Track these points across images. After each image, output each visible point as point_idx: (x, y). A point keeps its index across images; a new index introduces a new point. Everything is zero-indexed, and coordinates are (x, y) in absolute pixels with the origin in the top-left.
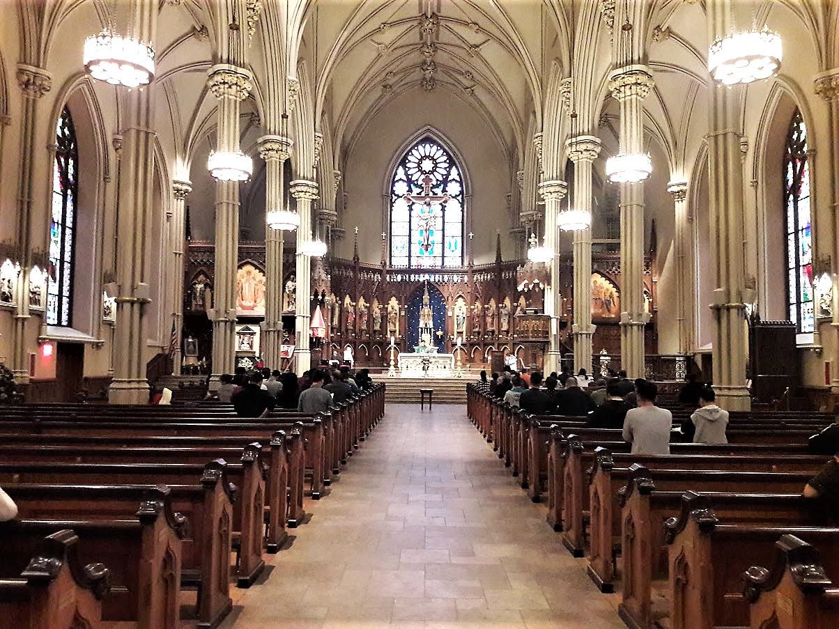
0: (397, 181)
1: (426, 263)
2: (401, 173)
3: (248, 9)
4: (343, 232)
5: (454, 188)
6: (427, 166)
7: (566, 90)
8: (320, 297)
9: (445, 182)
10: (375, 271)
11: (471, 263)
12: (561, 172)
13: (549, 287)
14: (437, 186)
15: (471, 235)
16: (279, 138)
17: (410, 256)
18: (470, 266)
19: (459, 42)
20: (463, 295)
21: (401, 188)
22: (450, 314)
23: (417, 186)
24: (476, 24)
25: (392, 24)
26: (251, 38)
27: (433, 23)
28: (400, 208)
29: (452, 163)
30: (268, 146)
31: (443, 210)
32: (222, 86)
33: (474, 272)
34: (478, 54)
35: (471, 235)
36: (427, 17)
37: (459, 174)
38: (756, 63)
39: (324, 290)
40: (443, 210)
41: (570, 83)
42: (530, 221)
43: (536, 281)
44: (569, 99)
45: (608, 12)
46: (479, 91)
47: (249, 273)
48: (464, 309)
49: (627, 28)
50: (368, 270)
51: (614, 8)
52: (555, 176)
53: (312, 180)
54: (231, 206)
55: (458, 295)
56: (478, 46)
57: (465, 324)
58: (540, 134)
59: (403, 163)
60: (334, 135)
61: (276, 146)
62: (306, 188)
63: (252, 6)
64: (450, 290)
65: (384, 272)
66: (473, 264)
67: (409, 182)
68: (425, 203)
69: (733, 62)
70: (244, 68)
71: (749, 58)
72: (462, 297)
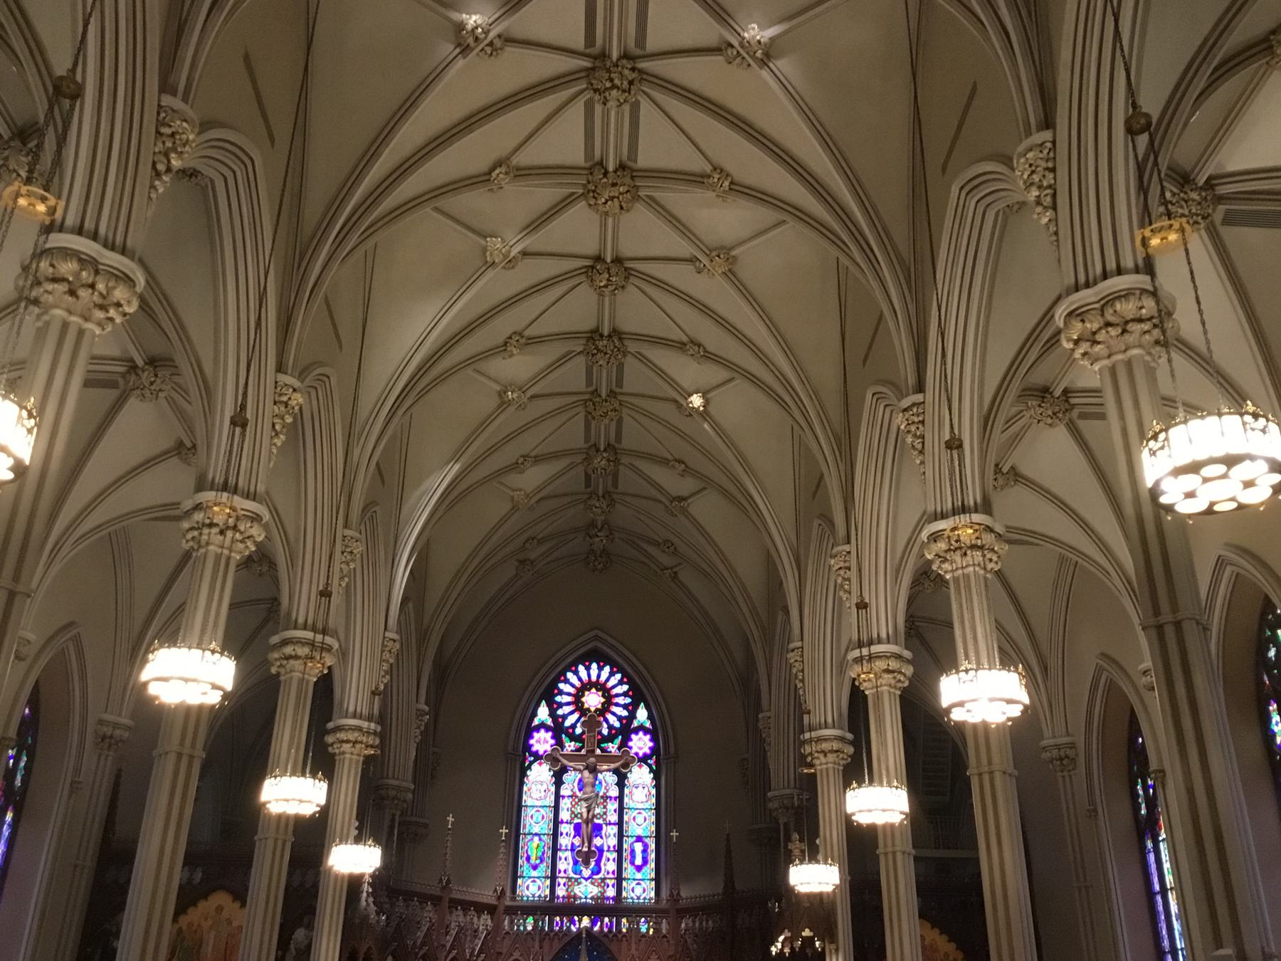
0: (537, 729)
1: (586, 891)
2: (543, 713)
3: (275, 403)
4: (425, 826)
5: (641, 744)
6: (593, 700)
7: (842, 564)
9: (626, 730)
10: (480, 908)
11: (675, 893)
12: (840, 715)
13: (833, 946)
14: (610, 739)
15: (674, 834)
16: (309, 635)
17: (553, 878)
18: (674, 898)
19: (655, 493)
21: (542, 742)
23: (573, 738)
24: (680, 462)
25: (538, 459)
26: (275, 451)
27: (609, 460)
28: (540, 775)
29: (637, 697)
30: (288, 650)
31: (621, 784)
32: (206, 531)
33: (682, 912)
34: (684, 511)
35: (674, 834)
36: (598, 450)
37: (650, 717)
38: (1242, 471)
39: (369, 948)
40: (621, 784)
41: (849, 553)
42: (787, 808)
43: (807, 933)
44: (849, 580)
45: (913, 428)
46: (686, 576)
47: (220, 909)
49: (954, 444)
50: (466, 906)
51: (922, 422)
52: (830, 720)
53: (370, 719)
54: (185, 760)
56: (681, 499)
58: (799, 644)
59: (549, 695)
60: (423, 638)
61: (303, 651)
62: (356, 734)
63: (285, 399)
64: (633, 951)
65: (501, 909)
66: (678, 894)
67: (558, 730)
68: (587, 768)
69: (1194, 468)
70: (254, 500)
71: (1231, 461)
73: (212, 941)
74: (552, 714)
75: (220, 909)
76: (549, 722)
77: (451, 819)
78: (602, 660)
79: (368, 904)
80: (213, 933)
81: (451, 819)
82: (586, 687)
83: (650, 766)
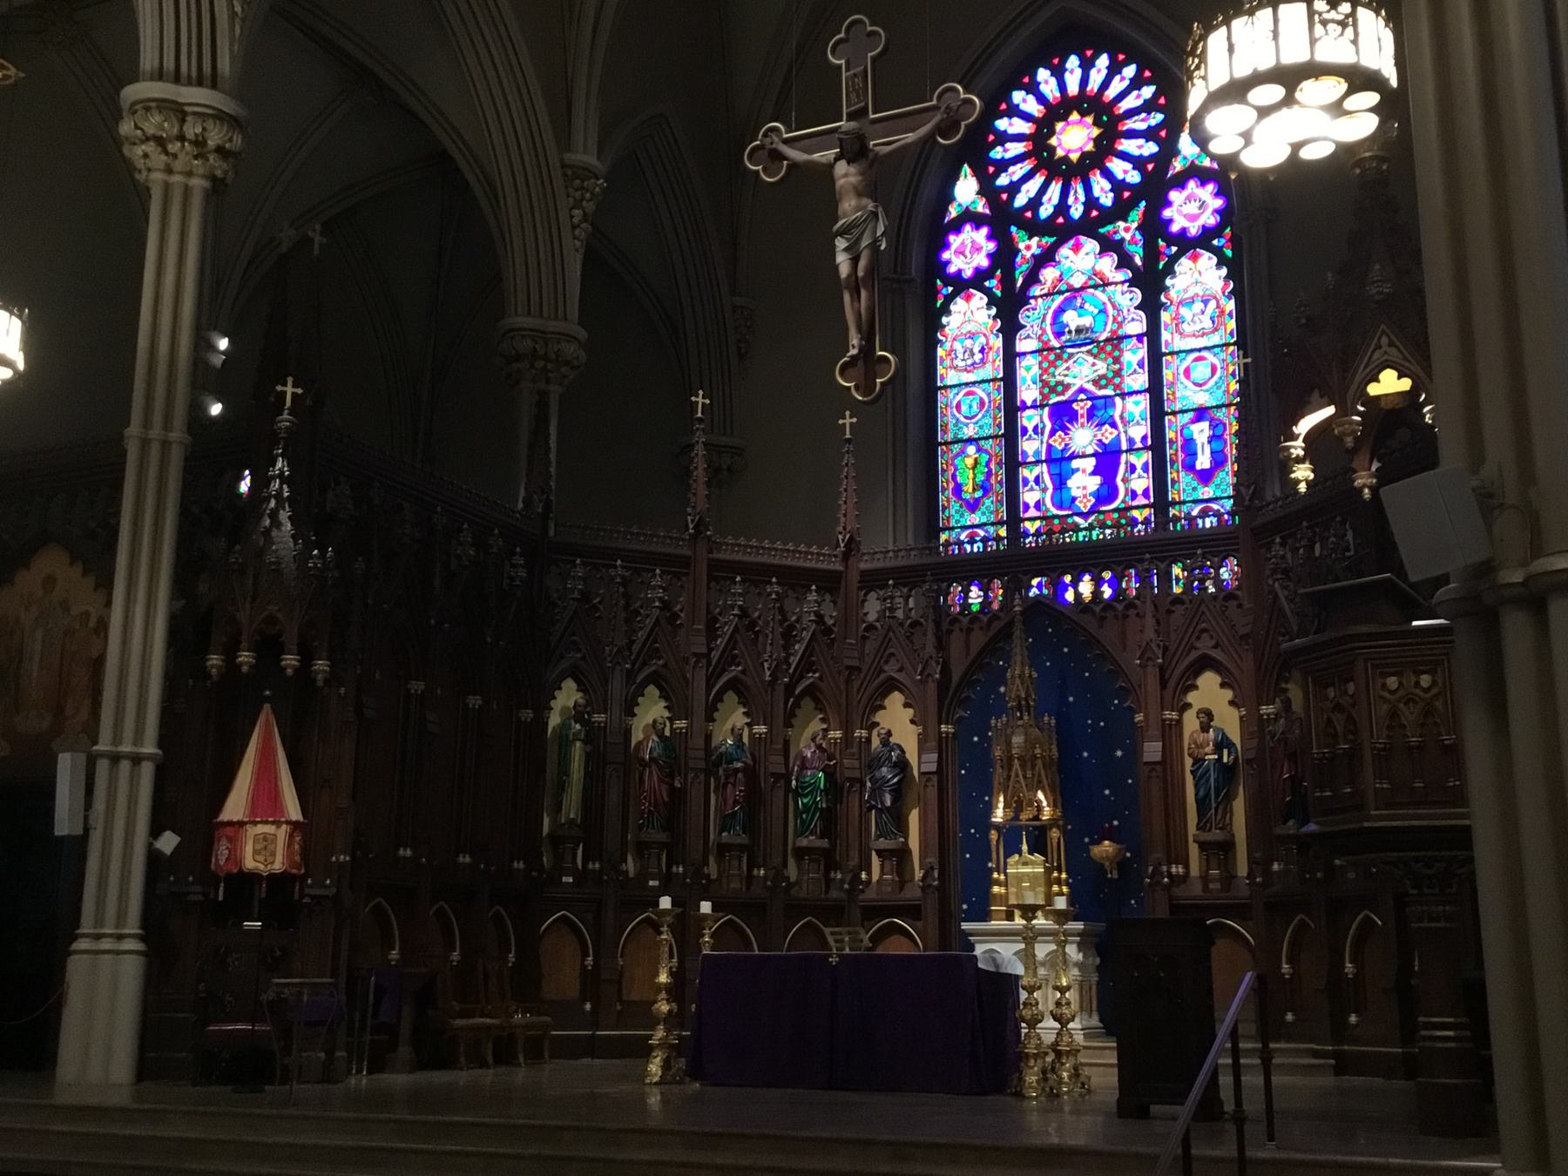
0: (956, 226)
2: (966, 190)
8: (290, 660)
14: (1120, 211)
20: (1217, 654)
21: (968, 251)
22: (1152, 750)
28: (969, 317)
31: (1152, 306)
40: (1152, 306)
47: (50, 581)
48: (1230, 721)
55: (1194, 655)
57: (1239, 805)
59: (976, 149)
72: (1217, 667)
73: (38, 647)
74: (987, 189)
75: (50, 581)
76: (981, 207)
77: (700, 399)
78: (1087, 43)
79: (276, 523)
80: (39, 634)
81: (700, 399)
82: (1057, 111)
83: (1217, 252)
